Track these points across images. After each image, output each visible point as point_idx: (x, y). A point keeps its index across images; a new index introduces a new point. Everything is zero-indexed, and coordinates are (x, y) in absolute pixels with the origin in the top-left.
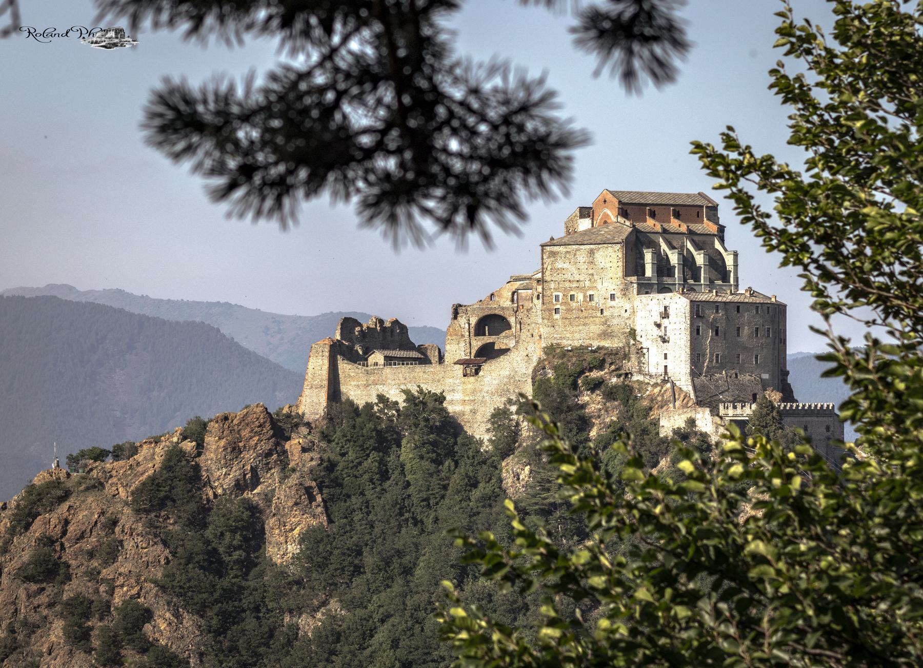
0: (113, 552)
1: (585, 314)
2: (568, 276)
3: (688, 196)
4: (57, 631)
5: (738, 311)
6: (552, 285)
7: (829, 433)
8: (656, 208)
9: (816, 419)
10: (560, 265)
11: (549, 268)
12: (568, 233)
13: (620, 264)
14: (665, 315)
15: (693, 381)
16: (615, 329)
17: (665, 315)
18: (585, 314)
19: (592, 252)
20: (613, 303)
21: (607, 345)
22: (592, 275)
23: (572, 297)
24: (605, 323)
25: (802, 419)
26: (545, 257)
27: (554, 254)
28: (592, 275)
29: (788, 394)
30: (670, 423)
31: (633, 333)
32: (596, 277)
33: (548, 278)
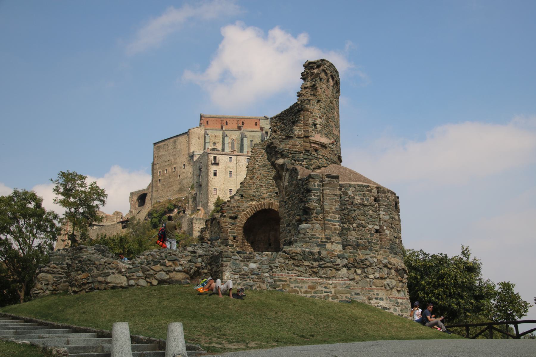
6: (158, 166)
16: (185, 186)
19: (175, 142)
20: (184, 170)
27: (159, 147)
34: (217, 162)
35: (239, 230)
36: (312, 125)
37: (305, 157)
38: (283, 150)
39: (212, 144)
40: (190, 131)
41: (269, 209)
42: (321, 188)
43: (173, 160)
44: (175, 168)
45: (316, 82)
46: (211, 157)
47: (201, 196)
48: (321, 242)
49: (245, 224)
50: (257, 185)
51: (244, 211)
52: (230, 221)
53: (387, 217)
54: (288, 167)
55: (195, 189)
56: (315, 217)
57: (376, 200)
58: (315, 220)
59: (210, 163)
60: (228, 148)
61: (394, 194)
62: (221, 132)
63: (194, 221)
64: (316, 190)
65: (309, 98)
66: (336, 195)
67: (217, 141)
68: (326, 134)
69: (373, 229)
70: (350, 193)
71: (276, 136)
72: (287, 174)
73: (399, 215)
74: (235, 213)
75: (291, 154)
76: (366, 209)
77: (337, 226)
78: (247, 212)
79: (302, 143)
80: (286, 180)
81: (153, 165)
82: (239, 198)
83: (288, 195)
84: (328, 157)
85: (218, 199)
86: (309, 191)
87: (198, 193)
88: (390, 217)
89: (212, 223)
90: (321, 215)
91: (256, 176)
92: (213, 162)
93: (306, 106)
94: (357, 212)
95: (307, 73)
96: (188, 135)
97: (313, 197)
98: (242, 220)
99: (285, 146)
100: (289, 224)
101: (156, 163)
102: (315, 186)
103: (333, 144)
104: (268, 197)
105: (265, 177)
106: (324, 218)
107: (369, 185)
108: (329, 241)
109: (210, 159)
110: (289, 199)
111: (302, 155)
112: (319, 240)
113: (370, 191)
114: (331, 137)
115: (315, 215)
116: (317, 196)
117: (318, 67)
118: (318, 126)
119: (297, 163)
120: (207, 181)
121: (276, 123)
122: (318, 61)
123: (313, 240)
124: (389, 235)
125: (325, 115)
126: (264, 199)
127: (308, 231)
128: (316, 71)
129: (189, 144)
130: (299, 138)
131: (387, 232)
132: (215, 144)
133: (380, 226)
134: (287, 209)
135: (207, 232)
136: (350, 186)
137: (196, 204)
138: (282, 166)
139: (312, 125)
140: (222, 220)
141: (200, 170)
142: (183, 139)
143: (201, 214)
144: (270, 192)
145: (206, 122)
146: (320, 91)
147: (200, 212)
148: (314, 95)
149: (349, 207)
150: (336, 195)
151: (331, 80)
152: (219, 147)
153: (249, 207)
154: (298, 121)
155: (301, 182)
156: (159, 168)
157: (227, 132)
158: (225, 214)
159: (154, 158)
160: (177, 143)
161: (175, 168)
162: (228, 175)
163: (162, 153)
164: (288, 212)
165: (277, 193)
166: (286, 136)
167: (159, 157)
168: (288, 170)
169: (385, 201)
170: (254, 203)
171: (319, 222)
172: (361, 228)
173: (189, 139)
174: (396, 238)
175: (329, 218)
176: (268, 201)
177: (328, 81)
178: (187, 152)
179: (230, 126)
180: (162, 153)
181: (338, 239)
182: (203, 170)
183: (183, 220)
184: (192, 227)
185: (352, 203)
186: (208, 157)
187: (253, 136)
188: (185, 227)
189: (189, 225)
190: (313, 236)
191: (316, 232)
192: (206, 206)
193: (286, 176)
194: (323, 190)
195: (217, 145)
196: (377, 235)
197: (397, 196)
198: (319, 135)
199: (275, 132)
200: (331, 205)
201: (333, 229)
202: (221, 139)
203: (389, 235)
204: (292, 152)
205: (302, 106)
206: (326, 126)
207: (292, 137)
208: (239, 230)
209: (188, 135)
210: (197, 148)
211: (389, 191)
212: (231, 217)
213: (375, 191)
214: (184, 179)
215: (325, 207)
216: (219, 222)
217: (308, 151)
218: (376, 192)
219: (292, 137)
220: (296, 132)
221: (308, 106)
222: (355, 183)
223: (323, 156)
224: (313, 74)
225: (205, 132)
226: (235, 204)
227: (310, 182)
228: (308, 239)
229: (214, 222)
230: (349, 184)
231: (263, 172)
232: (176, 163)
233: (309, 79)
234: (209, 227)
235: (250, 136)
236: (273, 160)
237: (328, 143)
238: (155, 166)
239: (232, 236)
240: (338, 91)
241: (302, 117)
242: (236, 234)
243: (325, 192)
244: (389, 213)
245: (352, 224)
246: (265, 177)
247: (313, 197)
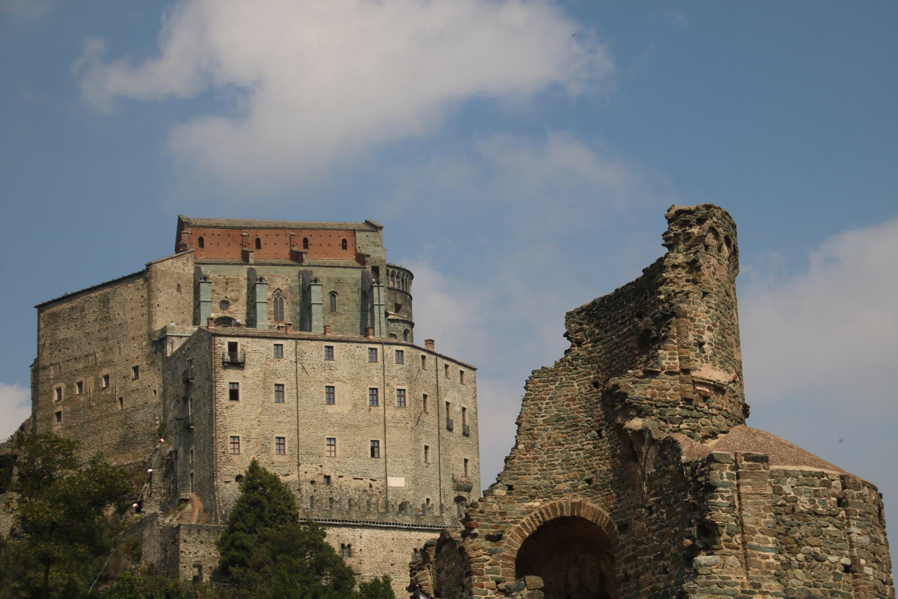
1: (97, 414)
6: (52, 372)
19: (105, 301)
20: (135, 384)
26: (42, 325)
27: (54, 316)
28: (107, 338)
34: (240, 357)
35: (508, 565)
36: (695, 345)
37: (685, 412)
38: (640, 400)
39: (217, 306)
40: (153, 268)
41: (573, 517)
42: (735, 482)
43: (100, 356)
44: (107, 378)
45: (699, 255)
46: (222, 345)
47: (193, 459)
48: (743, 592)
49: (519, 551)
50: (542, 463)
51: (515, 522)
52: (488, 545)
53: (865, 540)
54: (655, 437)
55: (171, 438)
56: (725, 541)
57: (841, 503)
58: (727, 547)
59: (219, 362)
60: (266, 316)
61: (875, 489)
62: (243, 271)
63: (183, 535)
64: (724, 485)
65: (686, 289)
66: (765, 496)
67: (231, 295)
68: (721, 363)
69: (839, 565)
70: (787, 489)
71: (581, 353)
72: (652, 450)
73: (885, 534)
74: (497, 527)
75: (657, 407)
76: (822, 521)
77: (772, 560)
78: (523, 524)
79: (678, 384)
80: (650, 463)
81: (37, 369)
82: (504, 493)
83: (655, 495)
84: (729, 411)
85: (254, 466)
86: (711, 488)
87: (181, 449)
88: (871, 537)
89: (438, 550)
90: (738, 536)
91: (539, 442)
92: (228, 358)
93: (681, 305)
94: (804, 529)
95: (676, 235)
96: (147, 280)
97: (719, 500)
98: (512, 543)
99: (643, 392)
100: (662, 555)
101: (45, 362)
102: (722, 478)
103: (734, 381)
104: (570, 491)
105: (560, 444)
106: (744, 543)
107: (826, 471)
108: (757, 591)
109: (219, 352)
110: (657, 502)
111: (678, 408)
112: (738, 588)
113: (827, 484)
114: (730, 368)
115: (725, 536)
116: (728, 498)
117: (700, 221)
118: (706, 346)
119: (671, 425)
120: (212, 415)
121: (581, 324)
122: (697, 209)
123: (727, 587)
124: (872, 578)
125: (718, 324)
126: (559, 494)
127: (715, 570)
128: (695, 230)
129: (150, 306)
130: (671, 373)
131: (868, 571)
132: (225, 304)
133: (852, 557)
134: (656, 523)
135: (426, 571)
136: (787, 474)
137: (174, 482)
138: (641, 434)
139: (695, 345)
140: (469, 544)
141: (187, 382)
142: (131, 293)
143: (191, 513)
144: (575, 478)
145: (195, 241)
146: (706, 273)
147: (189, 507)
148: (695, 282)
149: (787, 519)
150: (765, 496)
151: (725, 247)
152: (239, 313)
153: (525, 515)
154: (665, 338)
155: (688, 468)
156: (57, 379)
157: (260, 271)
158: (476, 531)
159: (40, 348)
160: (112, 304)
161: (107, 378)
162: (273, 397)
163: (64, 333)
164: (657, 530)
165: (589, 481)
166: (644, 372)
167: (56, 345)
168: (653, 441)
169: (859, 505)
170: (537, 504)
171: (734, 551)
172: (815, 562)
173: (150, 290)
174: (885, 583)
175: (755, 543)
176: (569, 499)
177: (720, 249)
178: (144, 331)
179: (268, 252)
180: (64, 333)
181: (775, 586)
182: (196, 382)
183: (146, 533)
184: (177, 552)
185: (793, 510)
186: (211, 344)
187: (339, 281)
188: (152, 554)
189: (164, 547)
190: (724, 582)
191: (730, 572)
192: (207, 488)
193: (650, 454)
194: (738, 486)
195: (233, 308)
196: (848, 578)
197: (879, 491)
198: (710, 365)
199: (579, 343)
200: (757, 517)
201: (763, 566)
202: (245, 291)
203: (872, 578)
204: (659, 404)
205: (671, 305)
206: (721, 345)
207: (657, 373)
208: (508, 565)
209: (147, 280)
210: (173, 318)
211: (865, 484)
212: (489, 538)
213: (837, 483)
214: (136, 409)
215: (745, 520)
216: (462, 549)
217: (689, 401)
218: (840, 486)
219: (657, 373)
220: (664, 362)
221: (684, 306)
222: (797, 468)
223: (719, 409)
224: (689, 236)
225: (197, 271)
226: (495, 507)
227: (712, 469)
228: (715, 586)
229: (444, 549)
230: (785, 471)
231: (554, 434)
233: (681, 246)
234: (432, 557)
235: (329, 279)
236: (619, 420)
237: (727, 380)
238: (42, 373)
239: (492, 579)
240: (736, 267)
241: (674, 331)
242: (500, 576)
243: (743, 490)
244: (869, 529)
245: (795, 554)
246: (560, 444)
247: (719, 500)
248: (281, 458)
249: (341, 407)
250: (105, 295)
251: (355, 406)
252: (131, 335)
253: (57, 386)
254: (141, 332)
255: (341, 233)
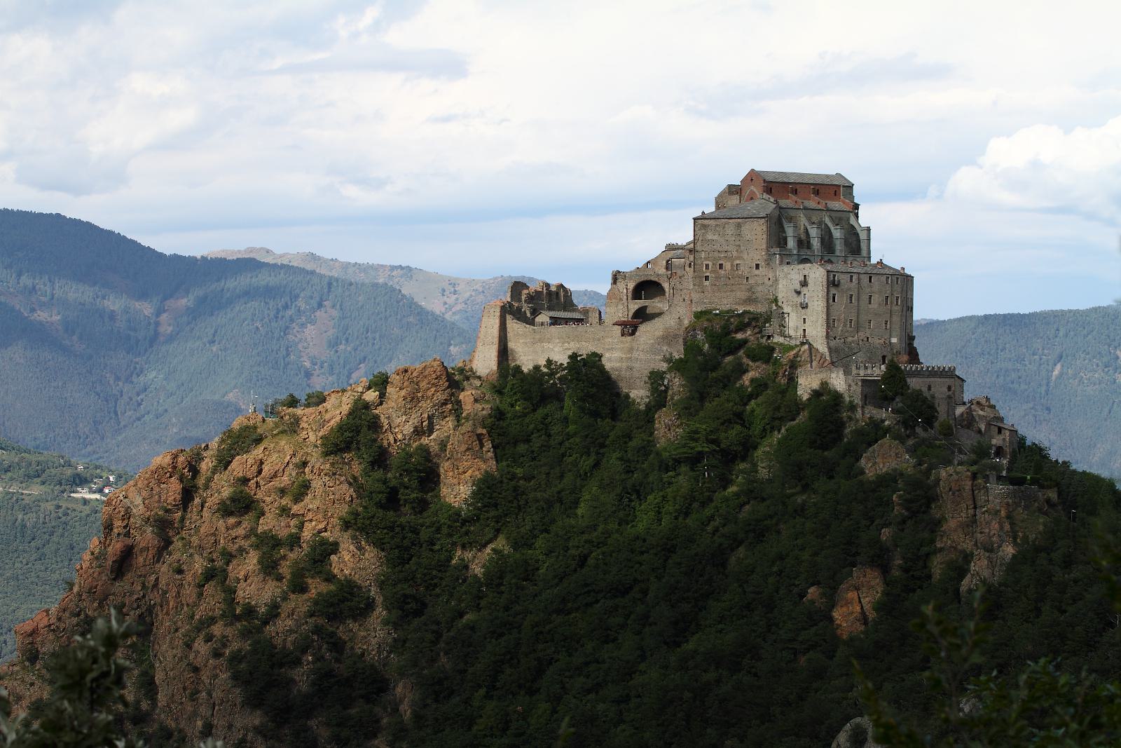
0: (303, 490)
1: (732, 281)
2: (717, 247)
3: (827, 176)
4: (252, 561)
5: (870, 281)
6: (703, 255)
7: (950, 393)
8: (798, 187)
9: (939, 379)
10: (710, 236)
11: (700, 239)
12: (718, 207)
13: (765, 236)
14: (804, 283)
15: (828, 343)
17: (804, 283)
18: (732, 281)
19: (739, 226)
20: (757, 272)
21: (752, 310)
22: (739, 246)
23: (721, 266)
24: (749, 290)
25: (926, 379)
27: (704, 227)
28: (739, 246)
29: (913, 356)
30: (807, 383)
31: (776, 300)
32: (742, 248)
33: (698, 248)
156: (706, 259)
232: (738, 258)
235: (836, 217)
248: (851, 329)
249: (874, 305)
250: (739, 224)
251: (880, 304)
252: (755, 247)
253: (707, 262)
254: (761, 248)
255: (835, 187)
